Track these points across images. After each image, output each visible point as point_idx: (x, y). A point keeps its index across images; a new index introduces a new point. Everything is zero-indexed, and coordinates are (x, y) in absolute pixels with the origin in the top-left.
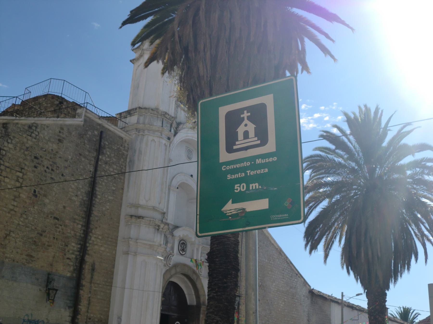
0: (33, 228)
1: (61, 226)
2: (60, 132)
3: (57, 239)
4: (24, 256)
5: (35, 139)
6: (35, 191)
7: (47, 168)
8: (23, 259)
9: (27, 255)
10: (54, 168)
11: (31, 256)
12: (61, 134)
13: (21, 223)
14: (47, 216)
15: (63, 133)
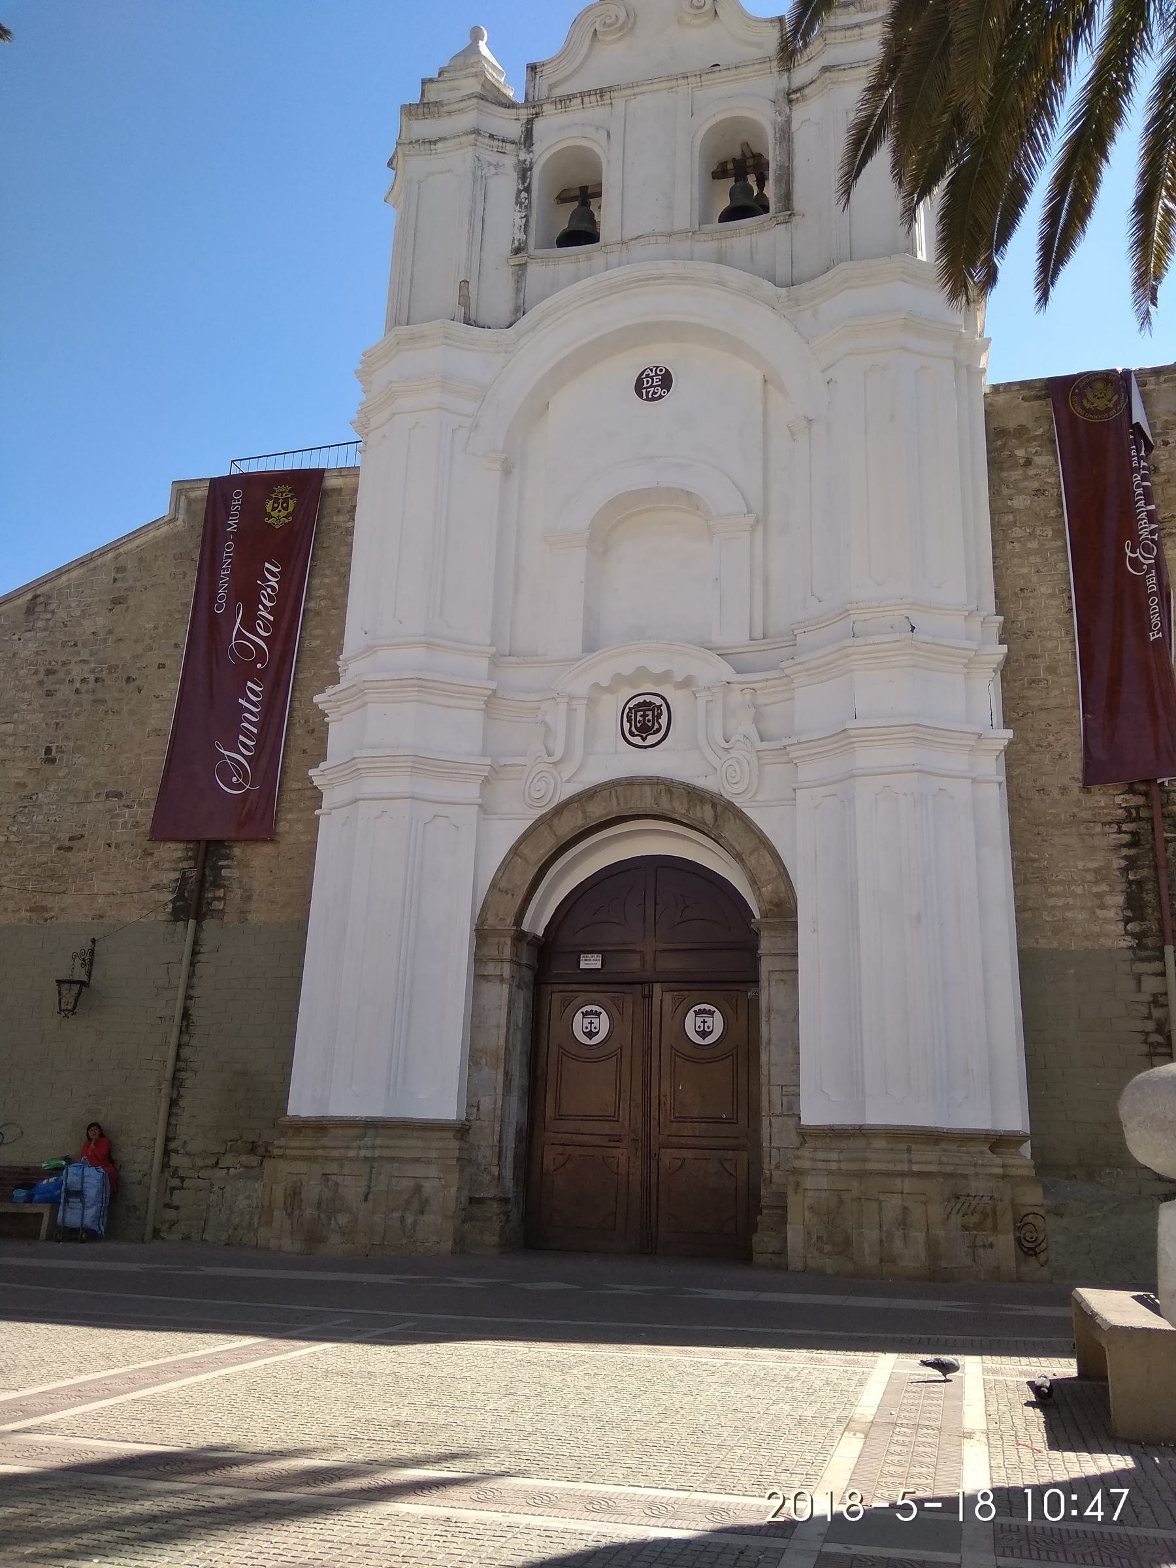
0: (46, 838)
1: (128, 807)
2: (115, 580)
3: (117, 846)
4: (23, 913)
5: (45, 630)
6: (48, 750)
7: (83, 681)
8: (20, 920)
9: (32, 910)
10: (104, 674)
11: (44, 909)
12: (117, 585)
13: (12, 838)
14: (87, 797)
15: (124, 579)
